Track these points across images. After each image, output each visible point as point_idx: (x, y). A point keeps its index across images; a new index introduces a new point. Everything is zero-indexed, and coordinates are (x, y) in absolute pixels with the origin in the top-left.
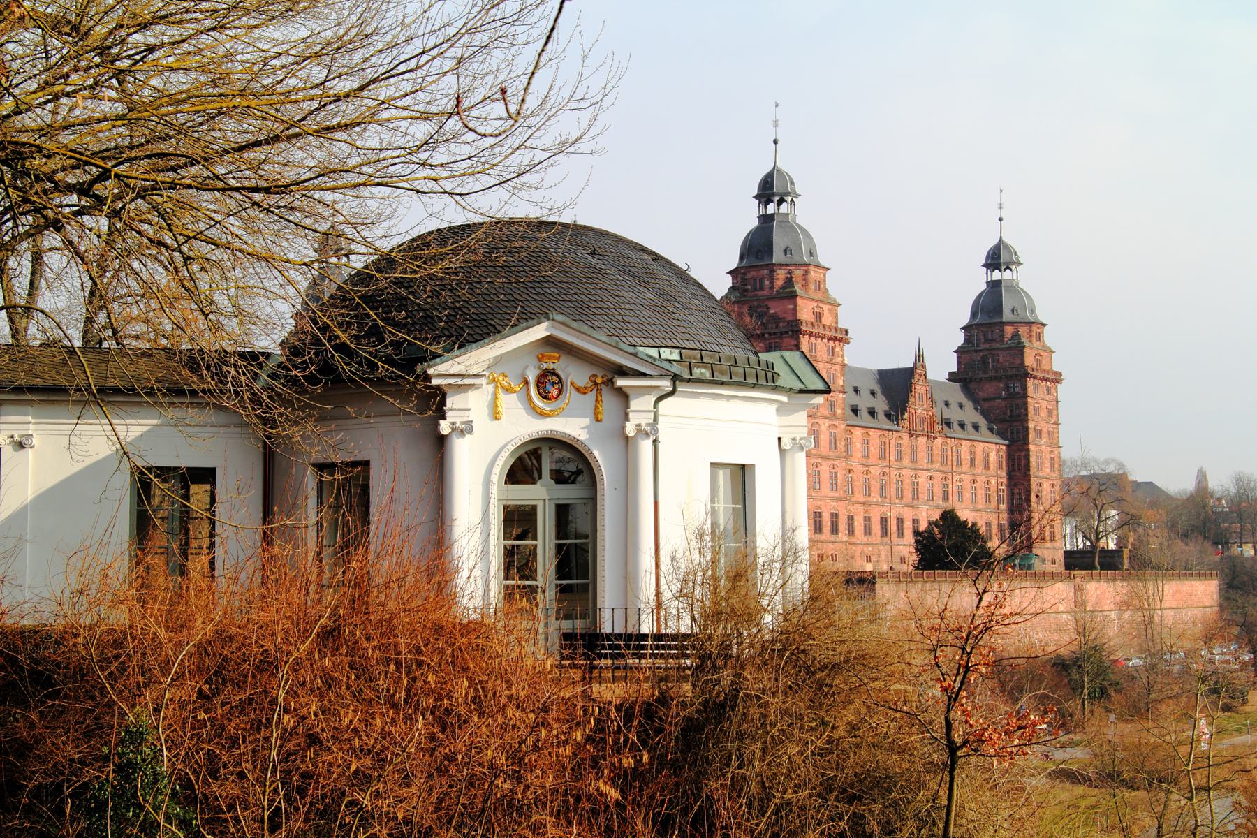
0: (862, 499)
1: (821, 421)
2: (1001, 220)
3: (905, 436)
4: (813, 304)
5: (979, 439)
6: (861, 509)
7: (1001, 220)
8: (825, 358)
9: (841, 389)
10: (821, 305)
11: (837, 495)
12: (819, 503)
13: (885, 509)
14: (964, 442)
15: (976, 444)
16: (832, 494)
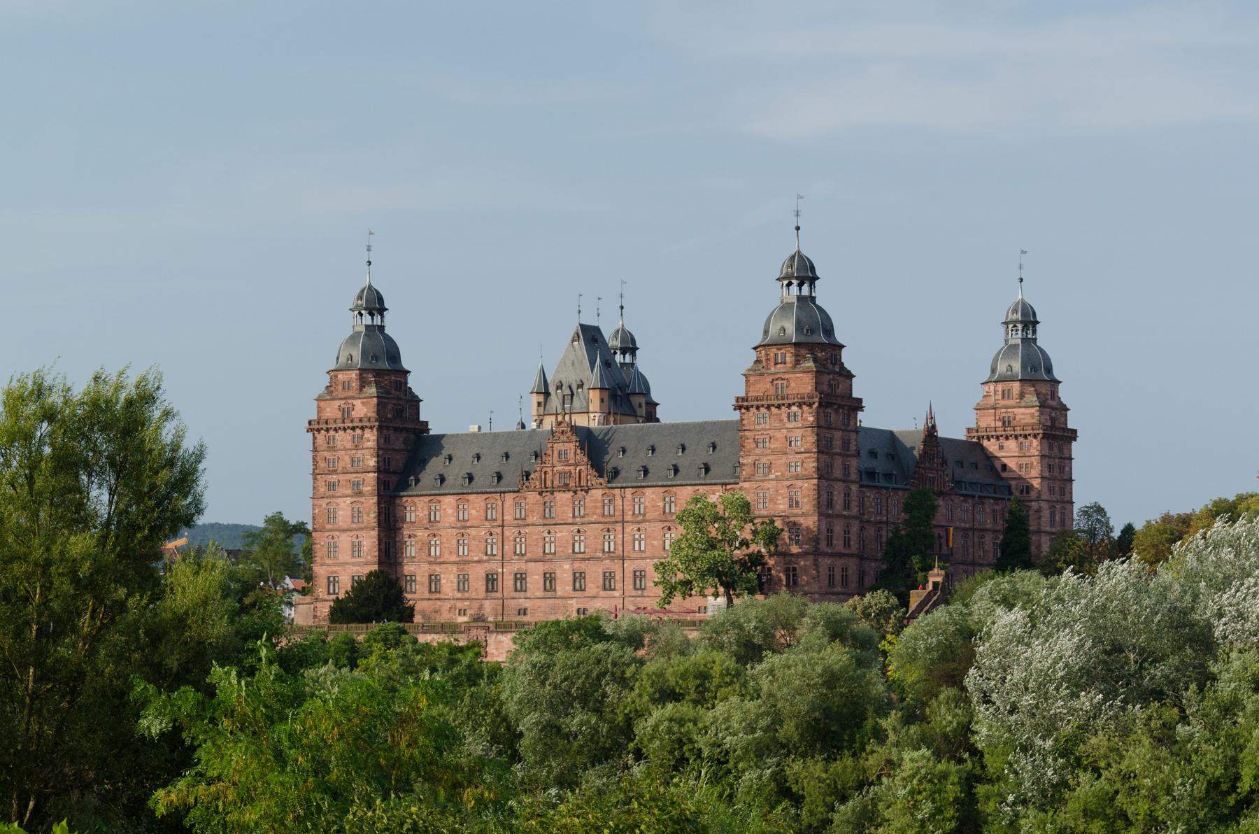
0: (453, 558)
1: (339, 501)
2: (798, 228)
3: (533, 497)
4: (338, 403)
5: (684, 483)
6: (454, 568)
7: (798, 228)
8: (349, 445)
9: (374, 469)
10: (350, 401)
11: (363, 560)
12: (335, 569)
13: (495, 567)
14: (648, 491)
15: (674, 489)
16: (354, 560)
